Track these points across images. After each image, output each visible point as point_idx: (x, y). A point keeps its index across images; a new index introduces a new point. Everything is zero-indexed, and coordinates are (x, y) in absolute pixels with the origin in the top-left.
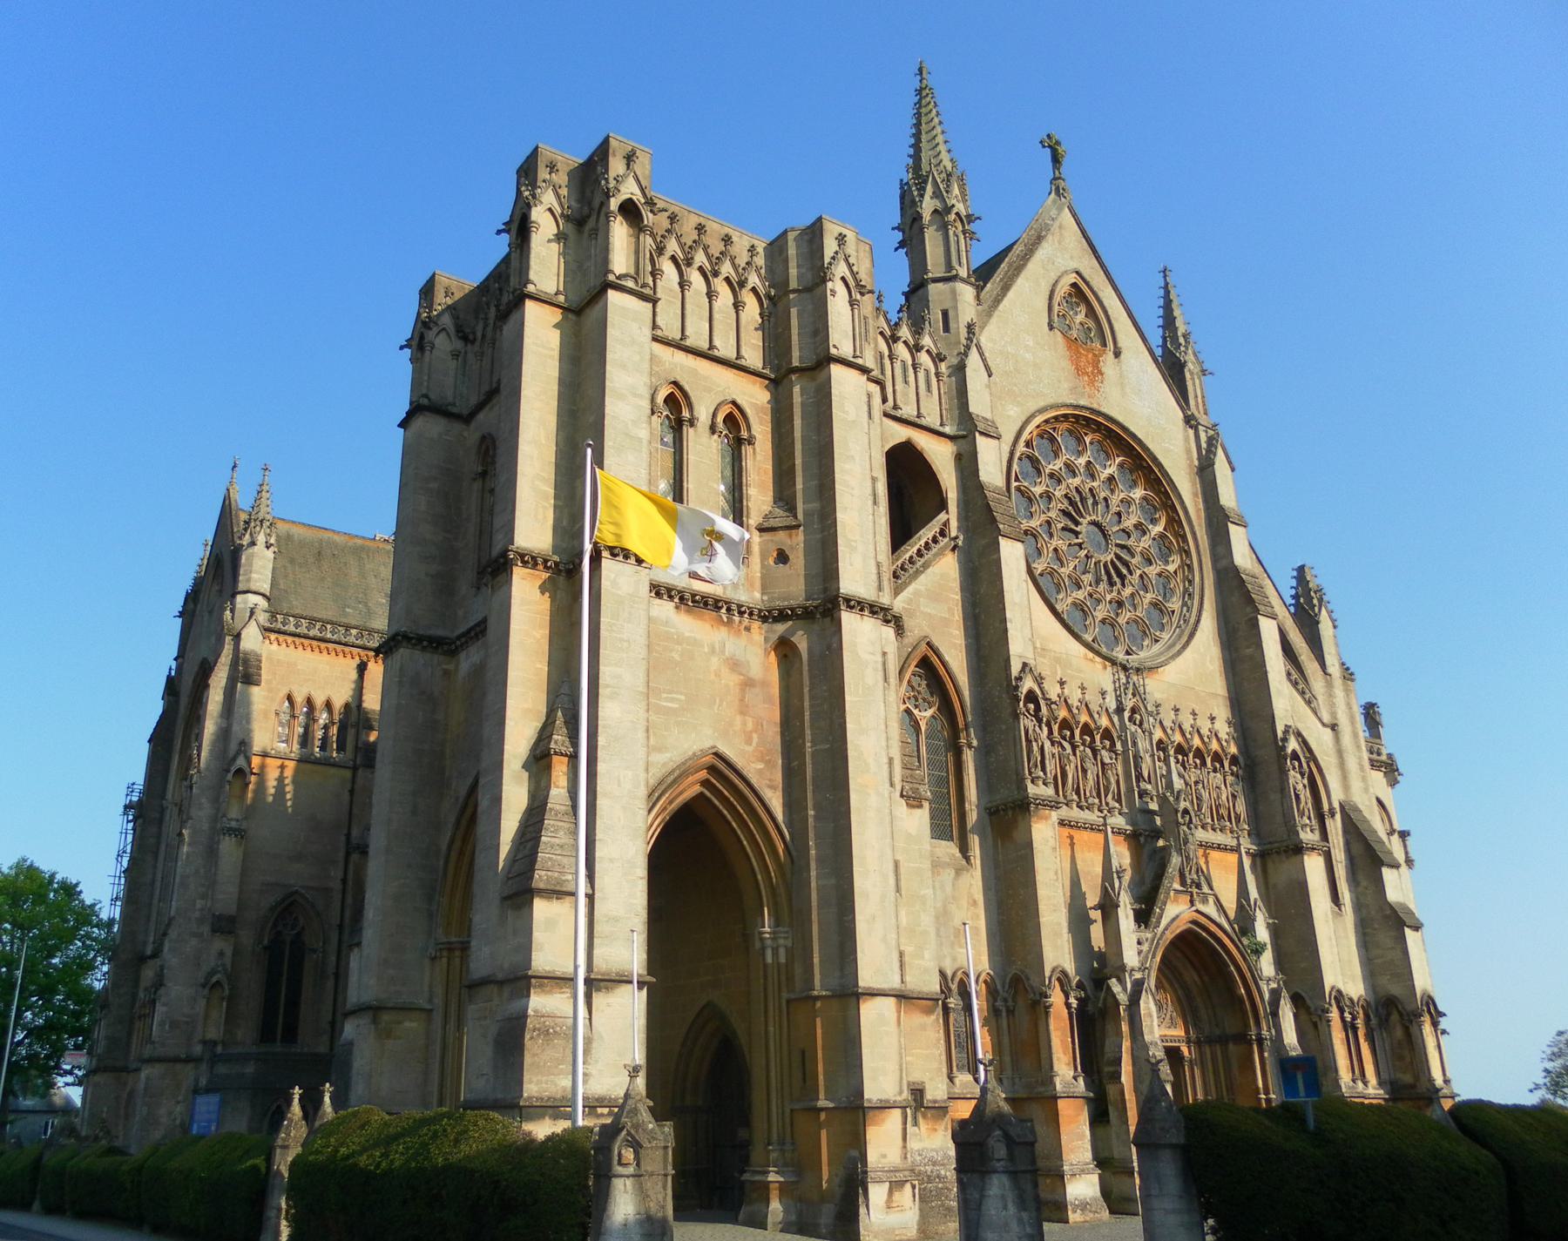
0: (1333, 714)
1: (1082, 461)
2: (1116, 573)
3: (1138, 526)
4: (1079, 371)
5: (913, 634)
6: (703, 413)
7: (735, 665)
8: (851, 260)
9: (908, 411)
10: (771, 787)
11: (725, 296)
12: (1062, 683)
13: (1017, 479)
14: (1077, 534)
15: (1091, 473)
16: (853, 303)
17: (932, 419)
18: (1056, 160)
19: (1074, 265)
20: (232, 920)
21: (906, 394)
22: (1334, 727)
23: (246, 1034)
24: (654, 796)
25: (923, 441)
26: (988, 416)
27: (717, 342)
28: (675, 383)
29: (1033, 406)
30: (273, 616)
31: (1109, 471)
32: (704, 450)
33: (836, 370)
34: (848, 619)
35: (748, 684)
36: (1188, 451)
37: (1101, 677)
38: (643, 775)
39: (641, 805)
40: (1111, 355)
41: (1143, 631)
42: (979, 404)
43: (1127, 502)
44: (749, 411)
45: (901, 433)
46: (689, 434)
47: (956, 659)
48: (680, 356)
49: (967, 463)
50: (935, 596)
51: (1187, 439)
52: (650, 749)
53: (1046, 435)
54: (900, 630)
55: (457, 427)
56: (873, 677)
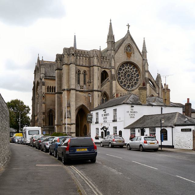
0: (159, 92)
1: (128, 67)
2: (131, 79)
3: (135, 74)
4: (128, 56)
5: (102, 92)
6: (82, 72)
7: (85, 96)
8: (97, 54)
9: (105, 67)
10: (88, 107)
11: (84, 58)
12: (121, 94)
13: (118, 71)
14: (126, 76)
15: (129, 68)
16: (97, 59)
17: (107, 67)
18: (129, 28)
19: (129, 42)
20: (45, 113)
21: (104, 65)
22: (158, 94)
23: (48, 124)
24: (76, 110)
25: (106, 70)
26: (114, 66)
27: (83, 64)
28: (79, 70)
29: (121, 63)
30: (45, 76)
31: (131, 68)
32: (82, 76)
33: (94, 67)
34: (94, 92)
35: (86, 98)
36: (143, 63)
37: (126, 92)
38: (75, 108)
39: (75, 111)
40: (133, 53)
41: (132, 86)
42: (113, 65)
43: (133, 71)
44: (87, 71)
45: (104, 70)
46: (80, 74)
47: (108, 93)
48: (79, 67)
49: (111, 71)
50: (106, 87)
51: (143, 62)
52: (76, 105)
53: (122, 65)
54: (101, 91)
55: (61, 71)
56: (97, 97)
